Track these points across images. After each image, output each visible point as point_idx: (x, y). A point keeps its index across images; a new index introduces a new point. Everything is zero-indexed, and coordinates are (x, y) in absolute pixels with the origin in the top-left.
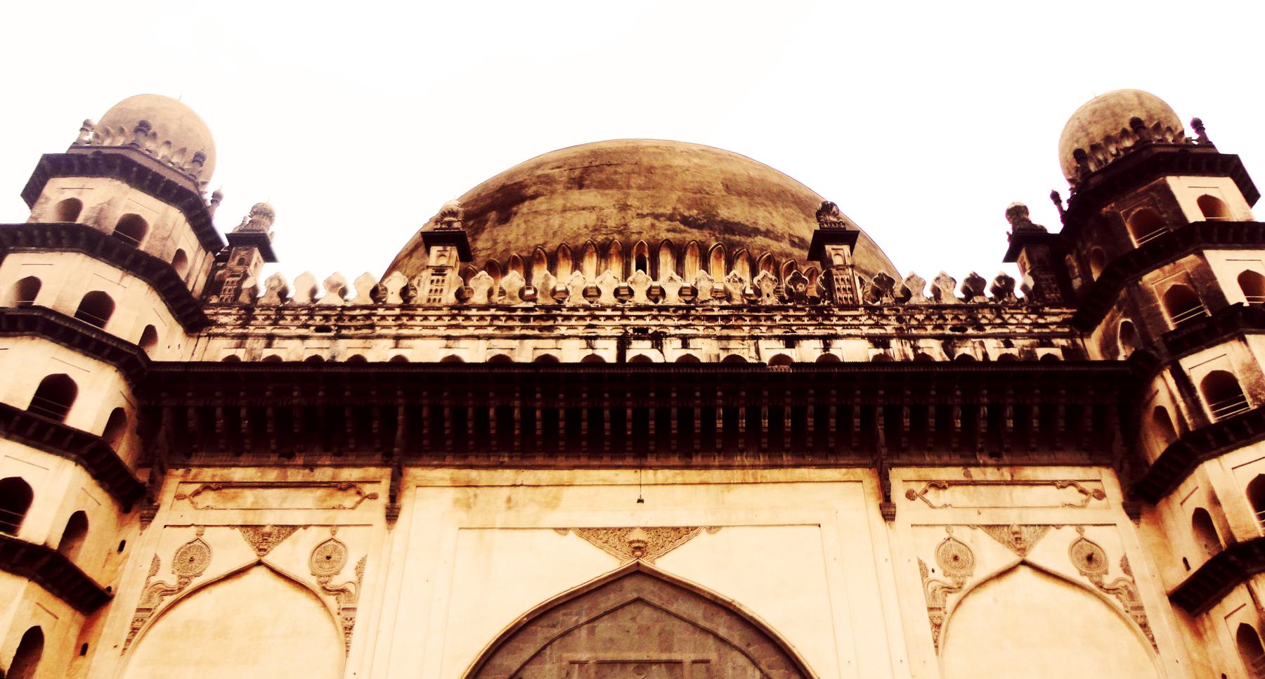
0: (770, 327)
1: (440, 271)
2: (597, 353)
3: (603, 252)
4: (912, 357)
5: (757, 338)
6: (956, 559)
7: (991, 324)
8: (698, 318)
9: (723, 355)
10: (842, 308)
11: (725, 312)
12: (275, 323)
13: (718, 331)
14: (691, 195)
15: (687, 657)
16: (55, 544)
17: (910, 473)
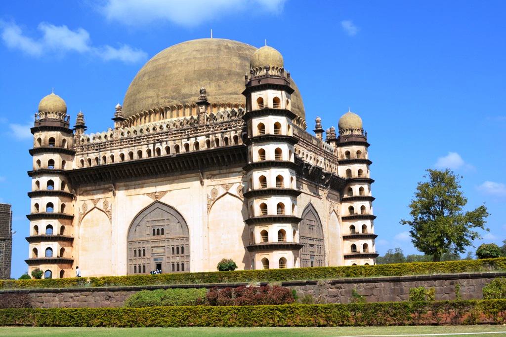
0: (185, 135)
1: (117, 129)
2: (150, 148)
4: (214, 140)
5: (181, 139)
6: (214, 193)
7: (234, 127)
8: (170, 135)
9: (174, 145)
10: (200, 127)
11: (175, 132)
12: (88, 150)
13: (174, 138)
14: (174, 87)
15: (165, 218)
16: (60, 211)
17: (208, 173)
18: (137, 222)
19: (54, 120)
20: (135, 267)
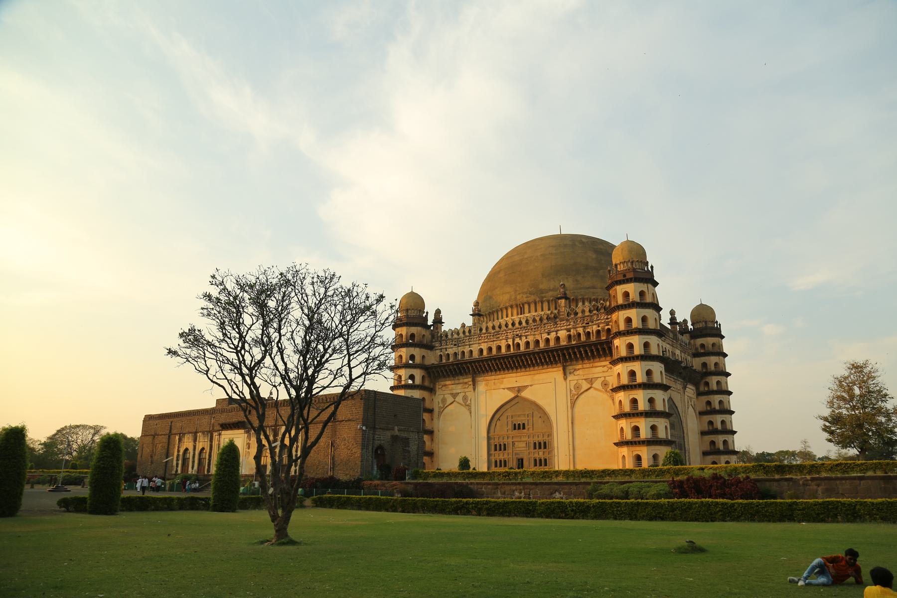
3: (512, 307)
6: (578, 387)
17: (571, 367)
18: (497, 416)
19: (413, 318)
20: (496, 462)
